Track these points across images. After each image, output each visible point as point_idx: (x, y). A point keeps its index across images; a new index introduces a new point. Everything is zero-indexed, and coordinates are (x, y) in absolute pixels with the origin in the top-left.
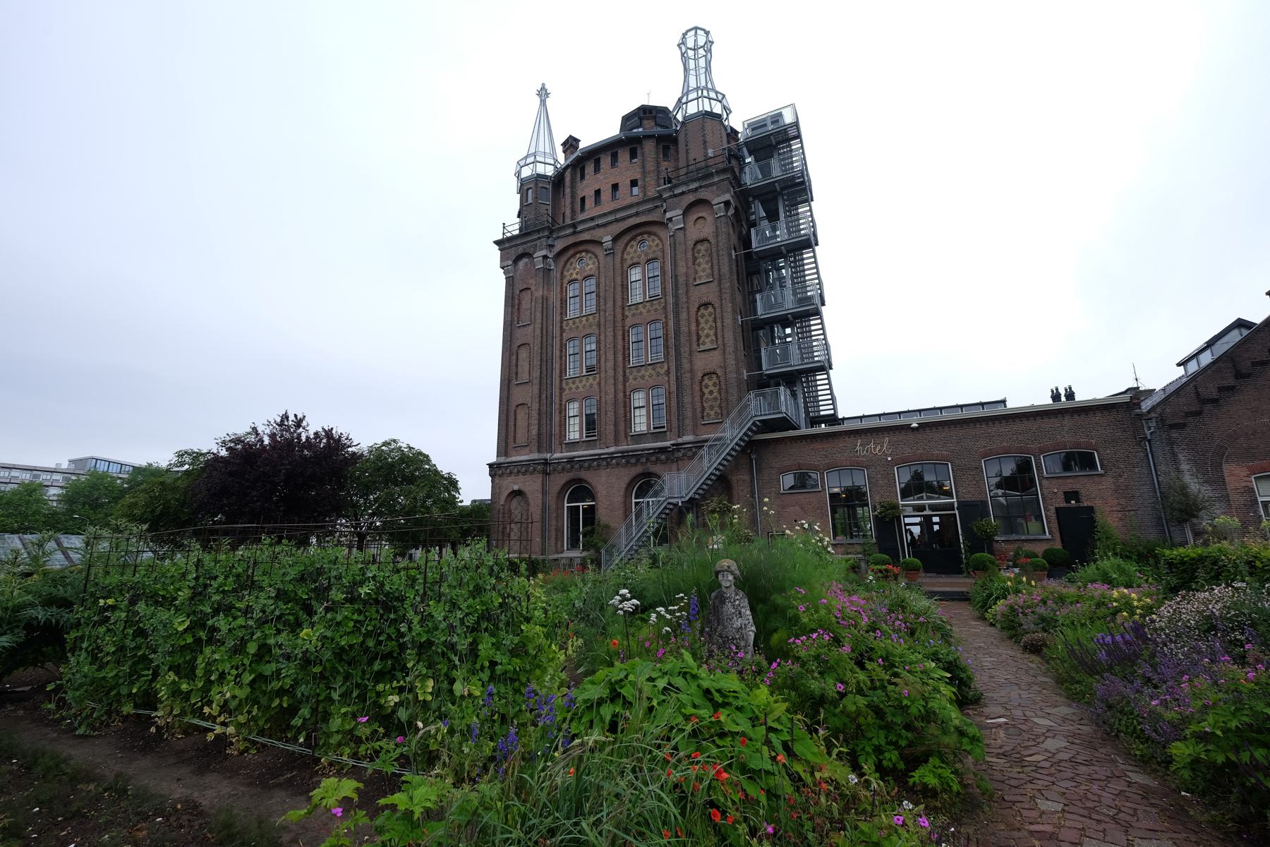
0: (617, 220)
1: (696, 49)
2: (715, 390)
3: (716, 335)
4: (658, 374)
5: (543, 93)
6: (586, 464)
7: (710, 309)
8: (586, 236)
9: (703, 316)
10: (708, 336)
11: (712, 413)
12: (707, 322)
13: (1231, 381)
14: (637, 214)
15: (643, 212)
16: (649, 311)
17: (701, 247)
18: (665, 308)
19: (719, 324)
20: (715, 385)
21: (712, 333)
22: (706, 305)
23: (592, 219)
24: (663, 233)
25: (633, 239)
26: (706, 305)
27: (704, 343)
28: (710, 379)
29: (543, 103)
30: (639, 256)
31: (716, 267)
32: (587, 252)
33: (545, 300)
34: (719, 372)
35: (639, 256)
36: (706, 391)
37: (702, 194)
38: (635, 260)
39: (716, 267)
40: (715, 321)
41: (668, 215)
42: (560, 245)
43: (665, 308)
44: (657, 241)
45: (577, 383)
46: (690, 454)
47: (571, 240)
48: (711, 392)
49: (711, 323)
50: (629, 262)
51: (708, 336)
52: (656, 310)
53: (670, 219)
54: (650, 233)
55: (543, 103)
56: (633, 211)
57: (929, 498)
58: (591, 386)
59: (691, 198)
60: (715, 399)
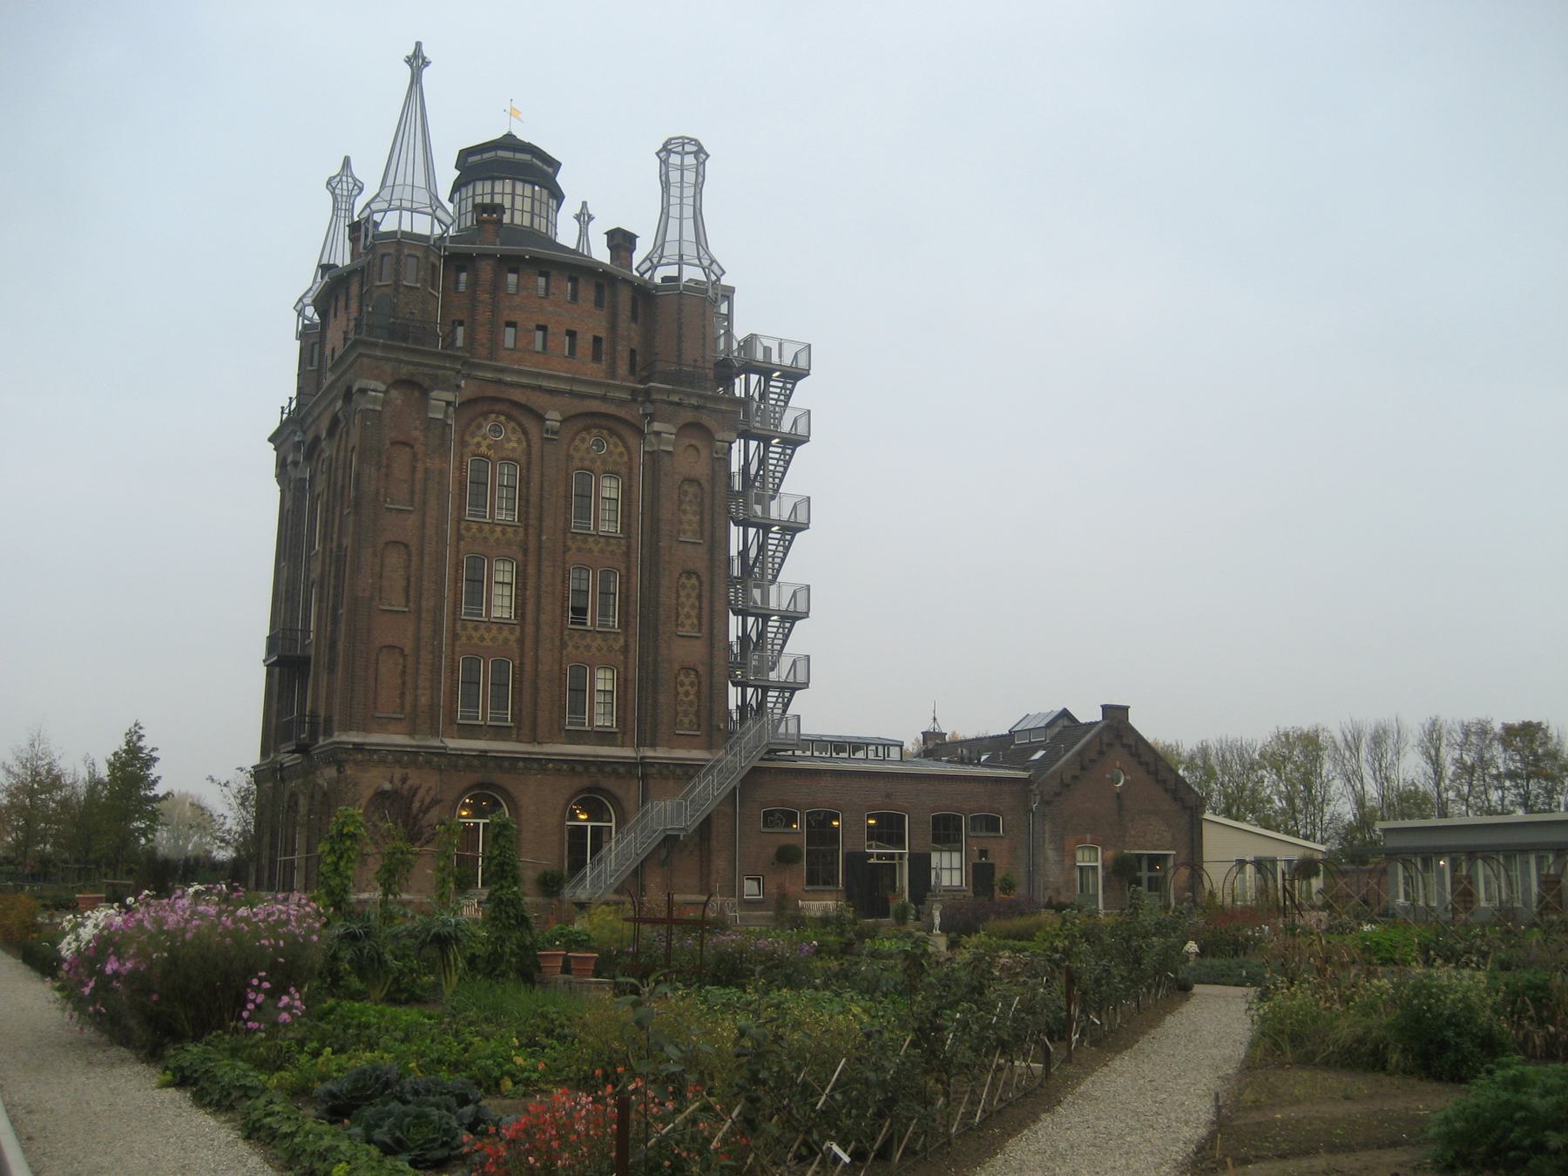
1: (682, 160)
2: (692, 691)
3: (699, 618)
4: (610, 649)
5: (417, 61)
6: (506, 764)
7: (694, 581)
8: (518, 395)
9: (684, 586)
10: (688, 616)
11: (686, 720)
12: (688, 596)
13: (1077, 773)
14: (604, 398)
15: (613, 400)
16: (602, 551)
17: (692, 489)
18: (627, 554)
19: (705, 604)
20: (692, 684)
21: (694, 613)
22: (689, 573)
23: (538, 375)
24: (632, 440)
25: (587, 429)
26: (689, 573)
27: (683, 625)
28: (687, 675)
29: (416, 80)
30: (593, 461)
31: (707, 526)
32: (509, 417)
33: (443, 473)
34: (701, 669)
35: (593, 461)
36: (681, 690)
37: (706, 420)
38: (587, 464)
39: (707, 526)
40: (700, 597)
41: (657, 426)
42: (468, 388)
43: (627, 554)
44: (621, 449)
45: (482, 631)
46: (665, 771)
47: (490, 391)
48: (687, 694)
49: (693, 600)
50: (577, 463)
51: (688, 616)
52: (613, 553)
53: (658, 434)
54: (612, 432)
55: (416, 80)
56: (599, 392)
57: (878, 847)
58: (506, 640)
59: (689, 416)
60: (691, 704)
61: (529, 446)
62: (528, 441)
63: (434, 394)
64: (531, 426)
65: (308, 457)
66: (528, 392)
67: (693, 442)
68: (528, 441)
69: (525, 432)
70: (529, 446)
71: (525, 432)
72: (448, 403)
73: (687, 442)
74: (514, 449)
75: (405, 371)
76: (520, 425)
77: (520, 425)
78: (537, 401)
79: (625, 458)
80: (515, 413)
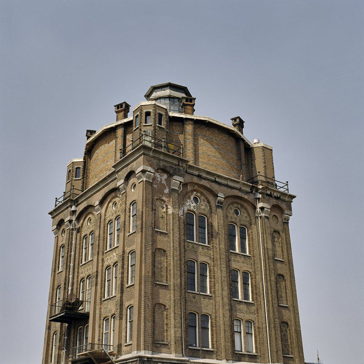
0: (227, 186)
25: (232, 203)
44: (246, 215)
61: (211, 209)
62: (210, 206)
63: (175, 177)
64: (211, 198)
65: (78, 219)
66: (210, 183)
67: (275, 214)
68: (210, 206)
69: (209, 202)
70: (211, 209)
71: (209, 202)
72: (181, 182)
73: (274, 213)
74: (204, 210)
75: (162, 164)
76: (206, 198)
77: (206, 198)
78: (215, 187)
79: (248, 219)
80: (205, 192)
